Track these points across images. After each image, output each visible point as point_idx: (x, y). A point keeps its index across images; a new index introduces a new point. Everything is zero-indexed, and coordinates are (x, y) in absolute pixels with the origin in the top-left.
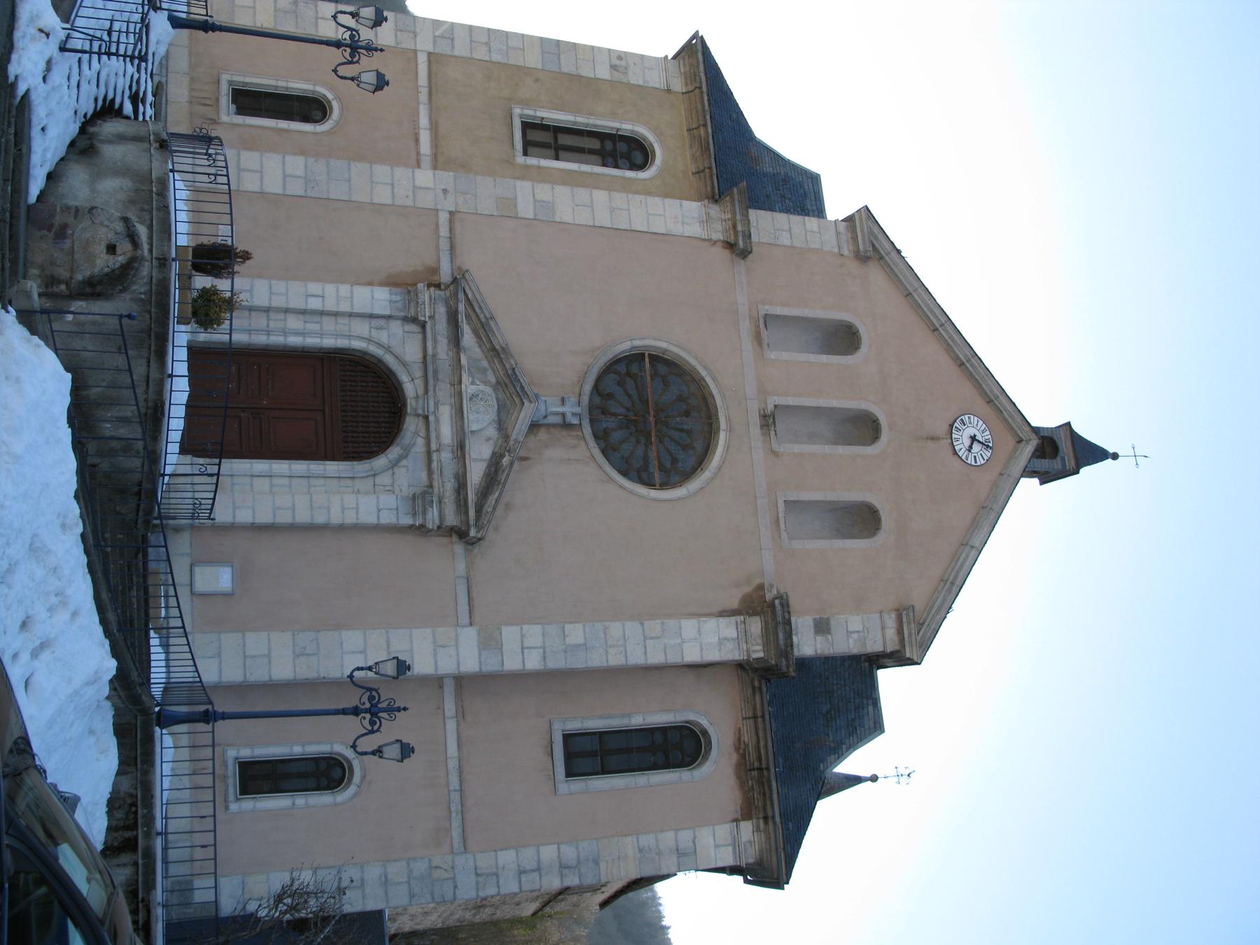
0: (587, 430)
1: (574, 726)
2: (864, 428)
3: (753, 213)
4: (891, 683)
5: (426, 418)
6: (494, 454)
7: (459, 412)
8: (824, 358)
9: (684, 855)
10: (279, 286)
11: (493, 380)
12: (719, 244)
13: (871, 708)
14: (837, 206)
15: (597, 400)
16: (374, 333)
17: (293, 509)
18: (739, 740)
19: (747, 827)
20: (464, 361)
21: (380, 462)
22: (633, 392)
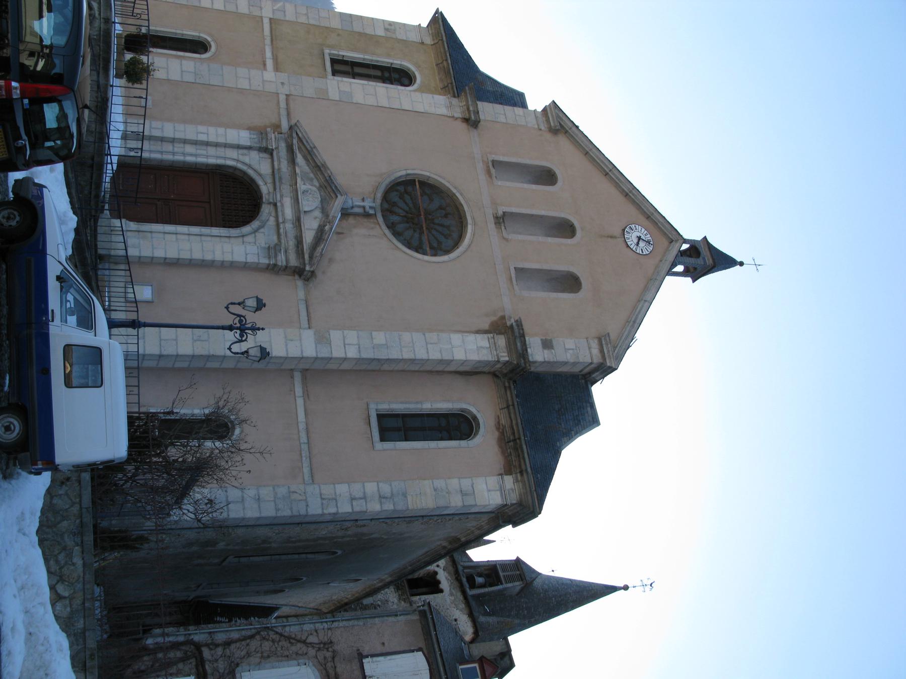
0: (380, 219)
1: (385, 407)
2: (565, 229)
3: (479, 103)
4: (599, 391)
5: (275, 205)
6: (320, 226)
7: (296, 200)
8: (534, 187)
9: (466, 495)
10: (180, 127)
11: (317, 185)
13: (589, 409)
14: (536, 103)
15: (386, 206)
17: (191, 250)
18: (499, 423)
19: (509, 481)
20: (298, 170)
21: (246, 229)
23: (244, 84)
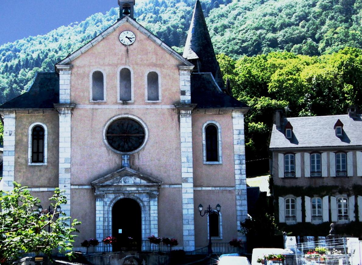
0: (131, 153)
1: (205, 159)
9: (240, 133)
12: (72, 112)
15: (120, 149)
17: (154, 224)
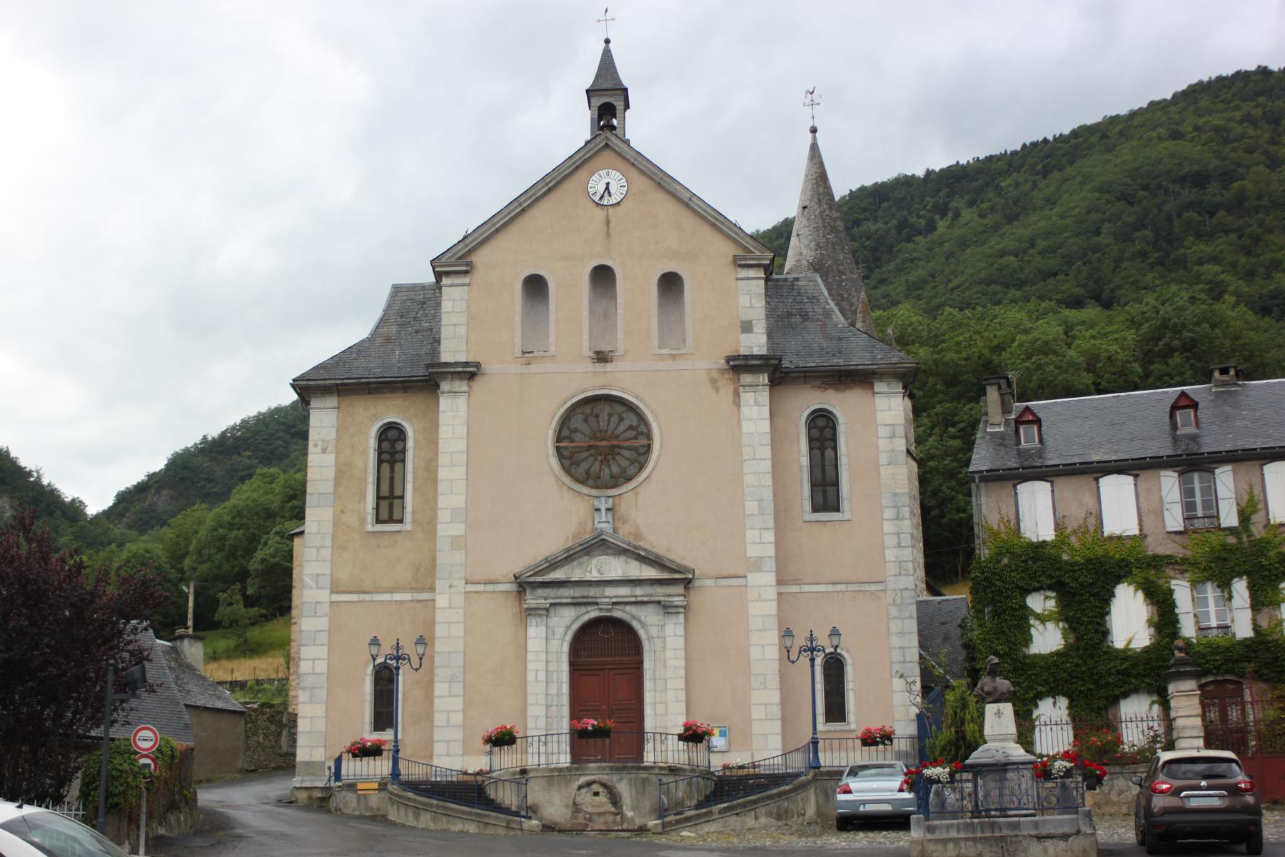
1: (807, 505)
2: (603, 276)
10: (531, 699)
15: (591, 482)
16: (557, 636)
22: (585, 455)
23: (458, 630)
